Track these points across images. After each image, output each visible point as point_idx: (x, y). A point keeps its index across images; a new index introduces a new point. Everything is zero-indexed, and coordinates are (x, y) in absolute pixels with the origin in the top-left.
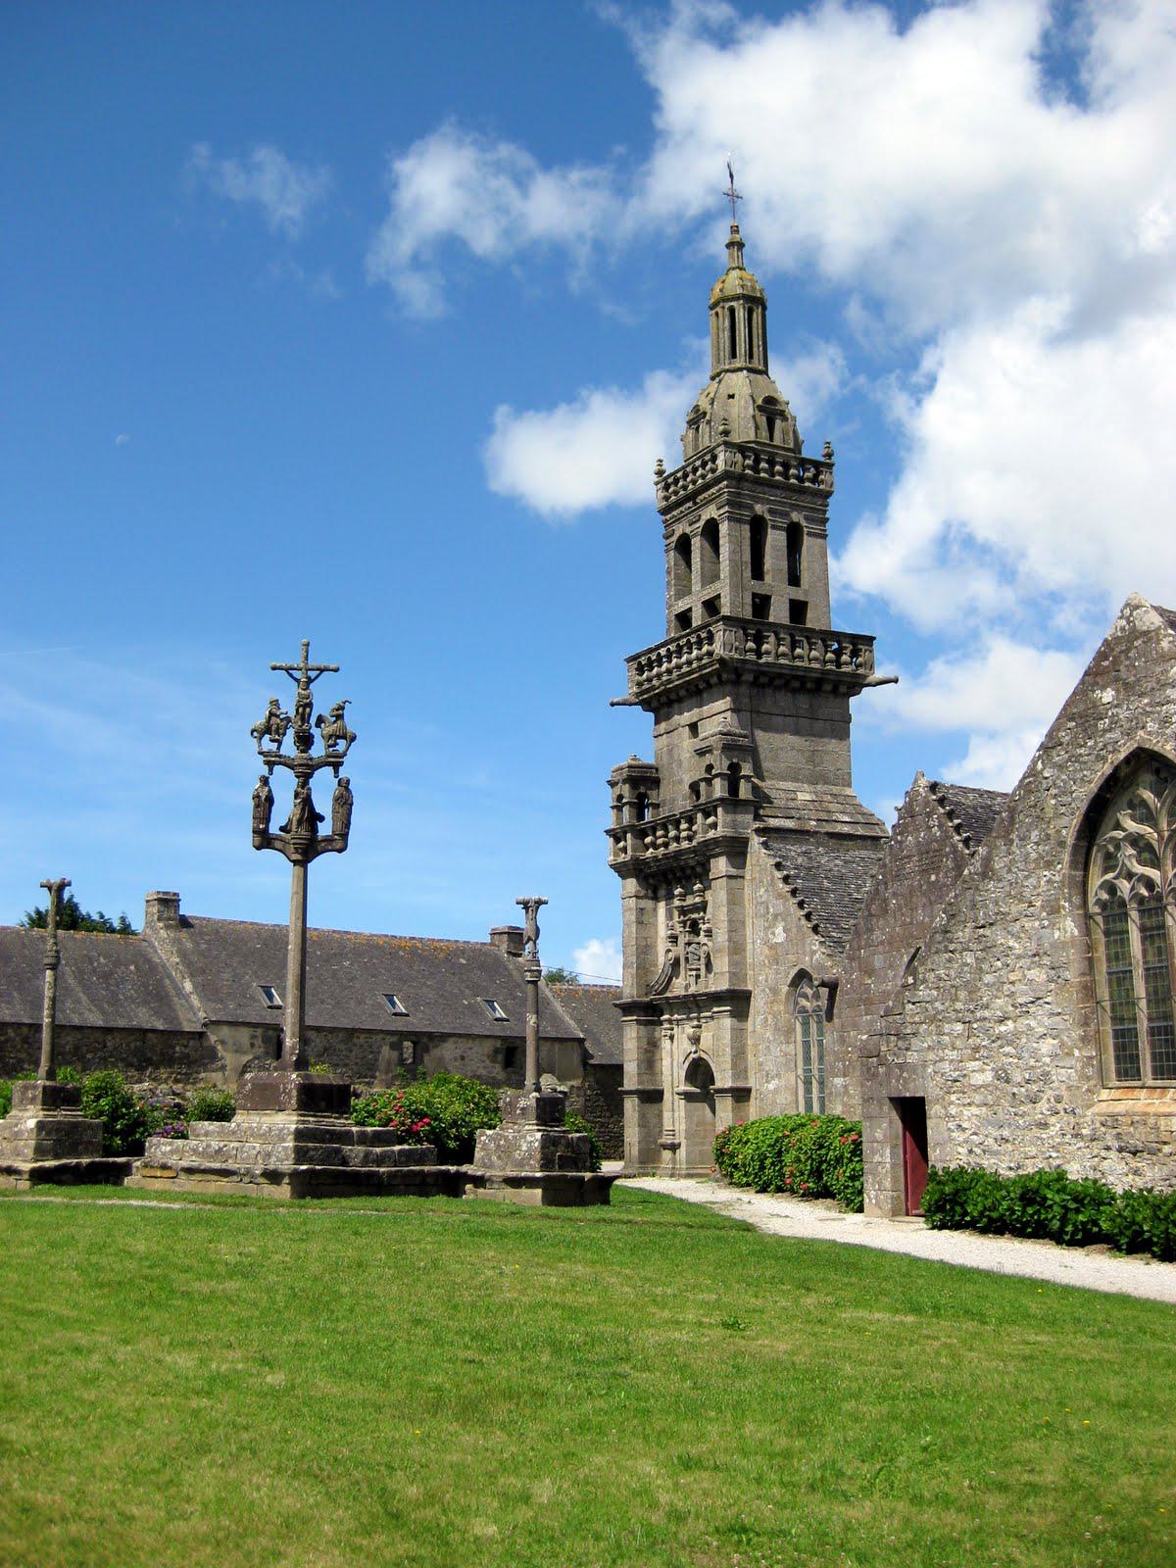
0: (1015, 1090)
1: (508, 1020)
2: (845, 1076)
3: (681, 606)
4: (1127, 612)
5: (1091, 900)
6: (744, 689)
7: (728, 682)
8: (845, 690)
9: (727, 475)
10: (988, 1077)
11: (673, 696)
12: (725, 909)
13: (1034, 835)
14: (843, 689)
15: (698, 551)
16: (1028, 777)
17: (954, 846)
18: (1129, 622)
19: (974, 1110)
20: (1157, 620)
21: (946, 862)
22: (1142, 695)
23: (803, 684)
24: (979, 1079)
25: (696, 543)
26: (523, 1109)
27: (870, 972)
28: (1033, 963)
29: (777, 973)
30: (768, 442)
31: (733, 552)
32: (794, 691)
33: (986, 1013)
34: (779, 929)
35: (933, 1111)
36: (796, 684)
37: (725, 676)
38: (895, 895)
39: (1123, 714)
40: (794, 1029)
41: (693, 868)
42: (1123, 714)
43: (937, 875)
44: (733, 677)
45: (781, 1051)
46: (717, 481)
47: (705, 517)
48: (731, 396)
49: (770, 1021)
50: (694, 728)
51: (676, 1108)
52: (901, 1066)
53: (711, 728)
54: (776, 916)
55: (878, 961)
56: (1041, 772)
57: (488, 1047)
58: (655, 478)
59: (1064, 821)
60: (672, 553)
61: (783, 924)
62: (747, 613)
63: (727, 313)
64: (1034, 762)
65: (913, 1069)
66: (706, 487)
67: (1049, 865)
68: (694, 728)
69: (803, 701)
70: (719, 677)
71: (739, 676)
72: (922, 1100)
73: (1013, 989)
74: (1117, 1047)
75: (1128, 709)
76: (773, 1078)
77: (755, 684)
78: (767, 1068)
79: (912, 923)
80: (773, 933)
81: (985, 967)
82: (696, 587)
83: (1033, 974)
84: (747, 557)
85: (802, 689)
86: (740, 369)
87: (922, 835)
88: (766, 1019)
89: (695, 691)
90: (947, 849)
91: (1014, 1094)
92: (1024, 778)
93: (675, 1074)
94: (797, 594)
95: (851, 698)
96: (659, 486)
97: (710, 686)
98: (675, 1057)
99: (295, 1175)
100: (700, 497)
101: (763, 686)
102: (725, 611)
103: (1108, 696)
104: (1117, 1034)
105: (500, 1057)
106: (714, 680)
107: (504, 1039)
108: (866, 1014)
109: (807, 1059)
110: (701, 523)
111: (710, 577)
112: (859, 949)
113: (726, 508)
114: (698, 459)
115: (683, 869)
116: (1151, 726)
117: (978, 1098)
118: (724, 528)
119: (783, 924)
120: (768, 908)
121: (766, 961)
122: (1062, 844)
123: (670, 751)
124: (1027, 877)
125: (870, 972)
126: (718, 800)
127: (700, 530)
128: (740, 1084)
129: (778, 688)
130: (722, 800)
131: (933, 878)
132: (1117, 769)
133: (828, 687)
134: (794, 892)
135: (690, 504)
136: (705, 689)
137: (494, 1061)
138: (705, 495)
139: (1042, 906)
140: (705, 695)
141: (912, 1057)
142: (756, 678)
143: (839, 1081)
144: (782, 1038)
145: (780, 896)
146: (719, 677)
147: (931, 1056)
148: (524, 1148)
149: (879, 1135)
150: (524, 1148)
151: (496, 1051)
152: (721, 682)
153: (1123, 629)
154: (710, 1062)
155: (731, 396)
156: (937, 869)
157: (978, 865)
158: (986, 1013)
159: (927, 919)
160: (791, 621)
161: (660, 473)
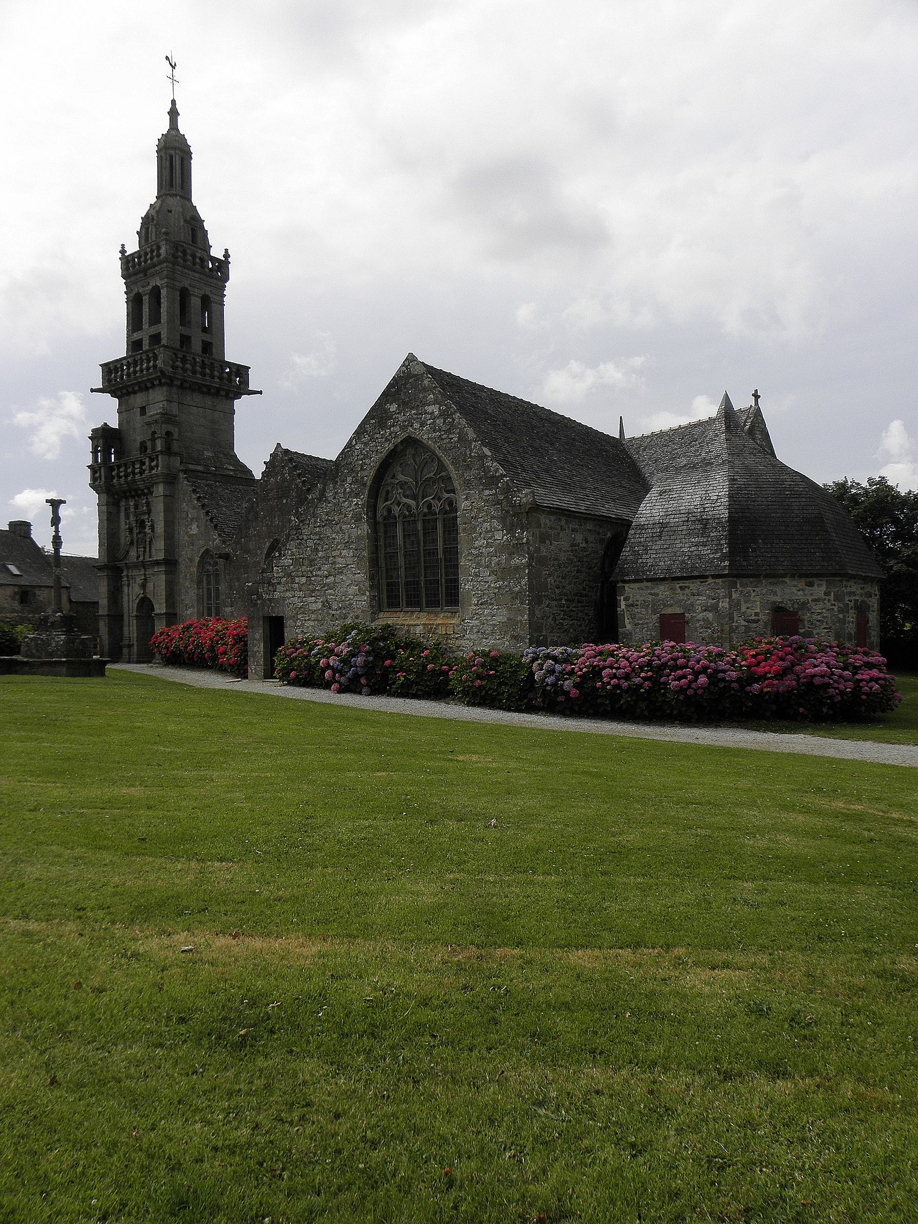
0: (334, 612)
1: (21, 576)
2: (231, 606)
3: (136, 336)
4: (407, 363)
5: (378, 515)
6: (174, 390)
7: (165, 384)
8: (233, 396)
9: (166, 260)
10: (319, 606)
11: (130, 389)
12: (162, 514)
13: (349, 479)
14: (231, 395)
15: (147, 305)
16: (347, 448)
17: (297, 485)
18: (407, 369)
19: (312, 623)
20: (423, 369)
22: (413, 408)
23: (209, 390)
24: (314, 607)
25: (146, 299)
26: (51, 623)
27: (247, 551)
28: (345, 546)
29: (193, 550)
30: (191, 243)
31: (169, 307)
32: (203, 393)
33: (319, 573)
34: (194, 526)
35: (289, 623)
36: (205, 389)
37: (163, 381)
38: (262, 510)
39: (401, 418)
40: (202, 581)
41: (142, 490)
42: (401, 418)
44: (168, 381)
46: (160, 263)
47: (153, 284)
48: (170, 212)
50: (143, 410)
51: (131, 624)
52: (269, 600)
53: (154, 410)
54: (192, 519)
55: (252, 545)
56: (354, 446)
57: (9, 591)
58: (120, 255)
59: (366, 473)
62: (177, 345)
63: (168, 158)
64: (351, 440)
65: (277, 601)
66: (154, 266)
67: (357, 496)
69: (208, 401)
70: (160, 381)
71: (172, 381)
72: (282, 618)
73: (334, 560)
74: (388, 591)
75: (404, 415)
76: (189, 608)
77: (181, 387)
79: (271, 525)
81: (320, 548)
82: (145, 326)
83: (344, 552)
84: (178, 312)
85: (208, 393)
86: (176, 195)
89: (145, 387)
91: (333, 615)
92: (345, 448)
93: (131, 606)
94: (207, 338)
95: (237, 402)
97: (153, 386)
98: (131, 597)
99: (108, 615)
101: (186, 389)
102: (164, 342)
103: (393, 407)
104: (388, 584)
105: (17, 597)
106: (156, 382)
107: (20, 586)
109: (209, 598)
111: (155, 319)
112: (241, 538)
113: (166, 280)
115: (136, 490)
116: (416, 425)
117: (313, 617)
118: (164, 292)
122: (365, 485)
123: (128, 422)
124: (344, 502)
125: (247, 551)
126: (159, 452)
128: (171, 611)
129: (193, 390)
130: (161, 452)
131: (284, 501)
132: (396, 447)
133: (223, 393)
134: (203, 506)
136: (151, 387)
137: (13, 599)
138: (153, 270)
139: (352, 517)
140: (150, 391)
141: (277, 595)
142: (182, 384)
143: (228, 609)
145: (194, 508)
146: (160, 381)
147: (288, 594)
148: (54, 645)
149: (257, 636)
150: (54, 645)
151: (15, 593)
152: (161, 384)
153: (404, 372)
155: (170, 212)
156: (287, 497)
157: (317, 494)
158: (319, 573)
160: (203, 352)
161: (123, 251)
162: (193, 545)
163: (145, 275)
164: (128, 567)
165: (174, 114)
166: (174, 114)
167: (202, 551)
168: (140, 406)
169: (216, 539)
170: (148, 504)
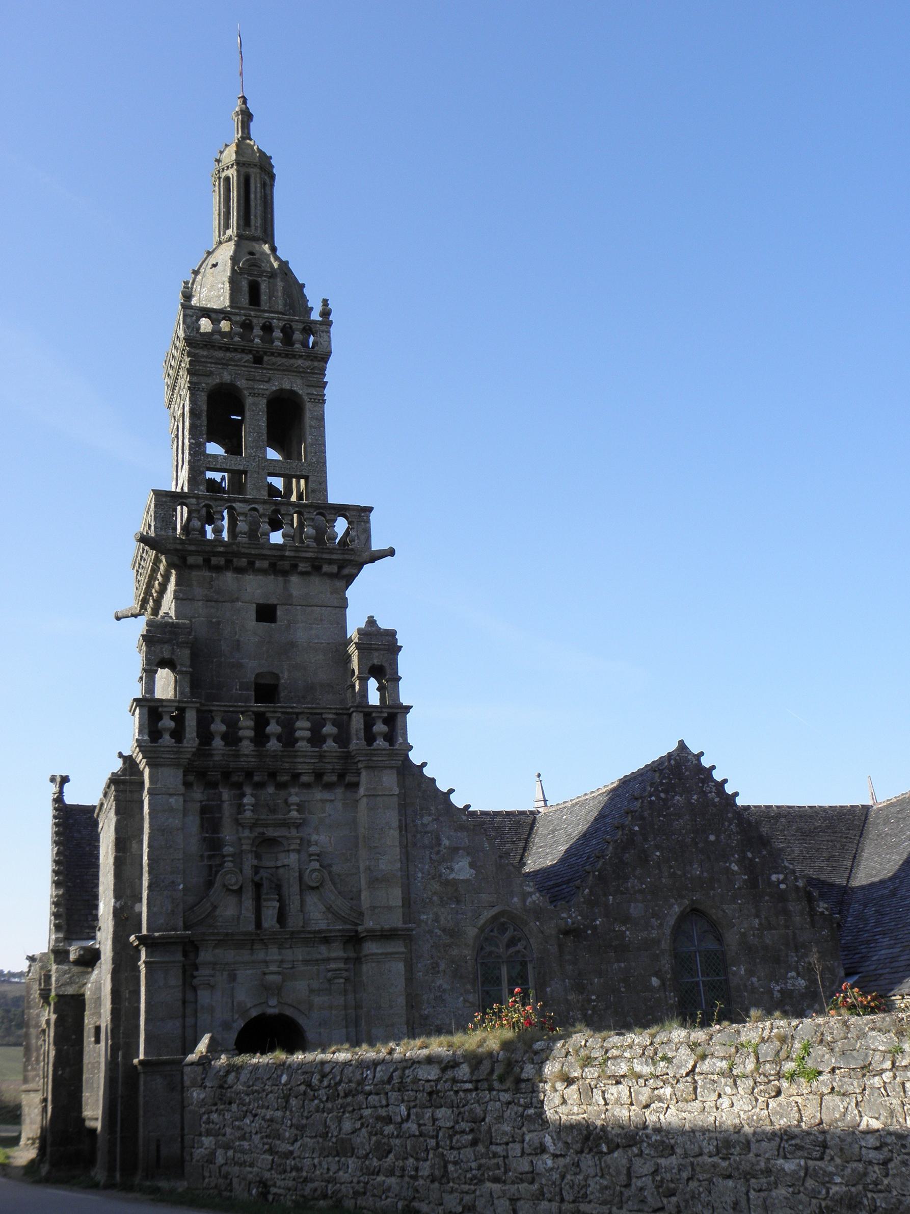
12: (395, 833)
21: (729, 826)
27: (626, 919)
38: (657, 847)
41: (296, 776)
43: (718, 837)
45: (465, 1001)
48: (286, 274)
49: (442, 966)
50: (266, 613)
55: (636, 910)
60: (203, 398)
61: (469, 859)
68: (266, 613)
70: (341, 568)
78: (438, 1022)
80: (452, 870)
87: (695, 797)
88: (435, 966)
90: (730, 815)
96: (189, 312)
100: (273, 359)
108: (619, 961)
110: (274, 387)
114: (279, 319)
119: (469, 859)
120: (438, 839)
121: (435, 898)
125: (626, 919)
127: (267, 393)
135: (250, 357)
138: (280, 361)
144: (469, 987)
154: (301, 1021)
159: (705, 874)
162: (458, 902)
163: (258, 360)
164: (226, 940)
165: (246, 117)
166: (246, 117)
167: (487, 915)
168: (261, 601)
169: (530, 894)
170: (300, 808)
